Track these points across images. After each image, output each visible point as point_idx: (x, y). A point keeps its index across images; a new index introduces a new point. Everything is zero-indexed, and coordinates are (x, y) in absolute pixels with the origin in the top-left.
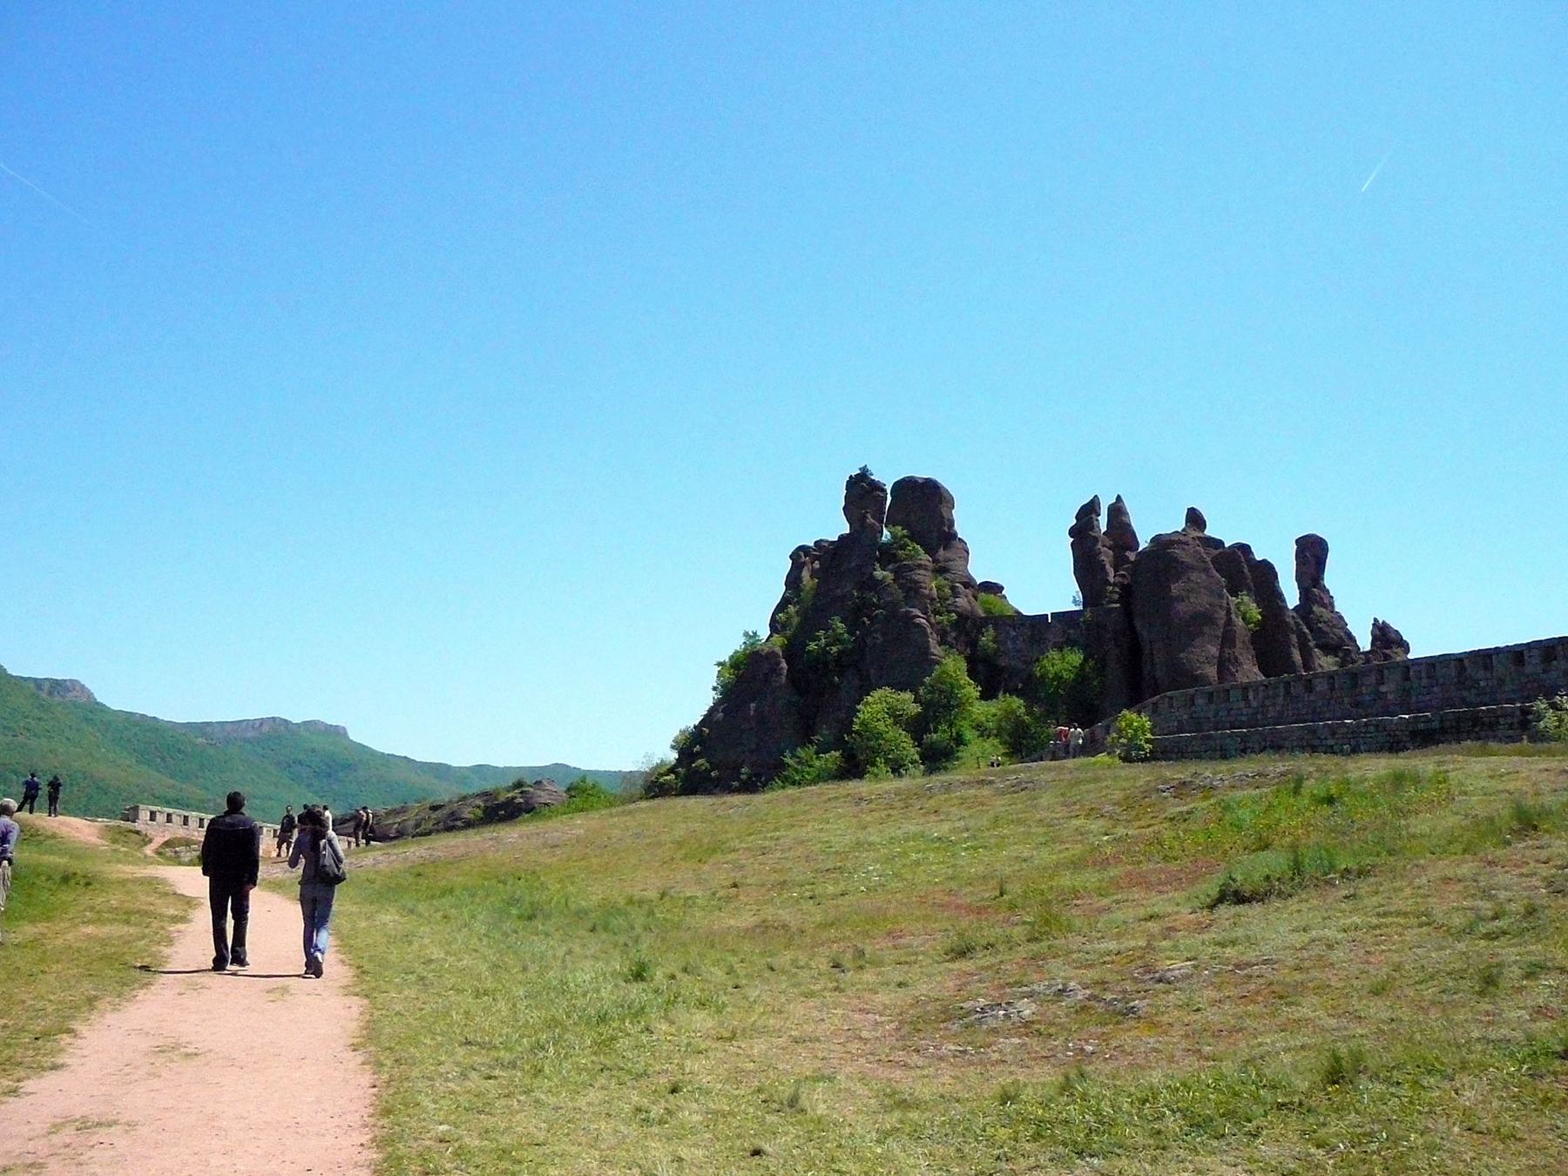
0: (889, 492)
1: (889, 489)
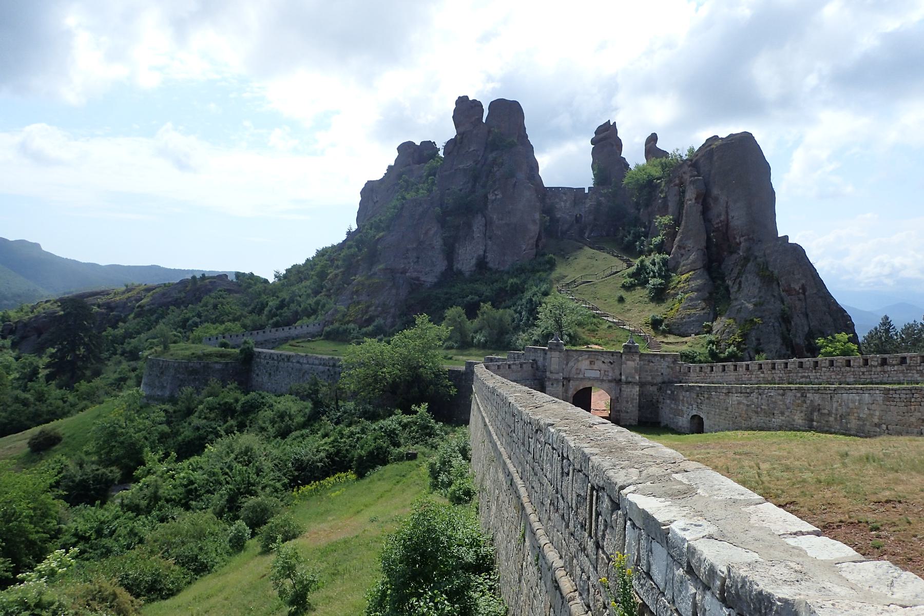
1: (486, 107)
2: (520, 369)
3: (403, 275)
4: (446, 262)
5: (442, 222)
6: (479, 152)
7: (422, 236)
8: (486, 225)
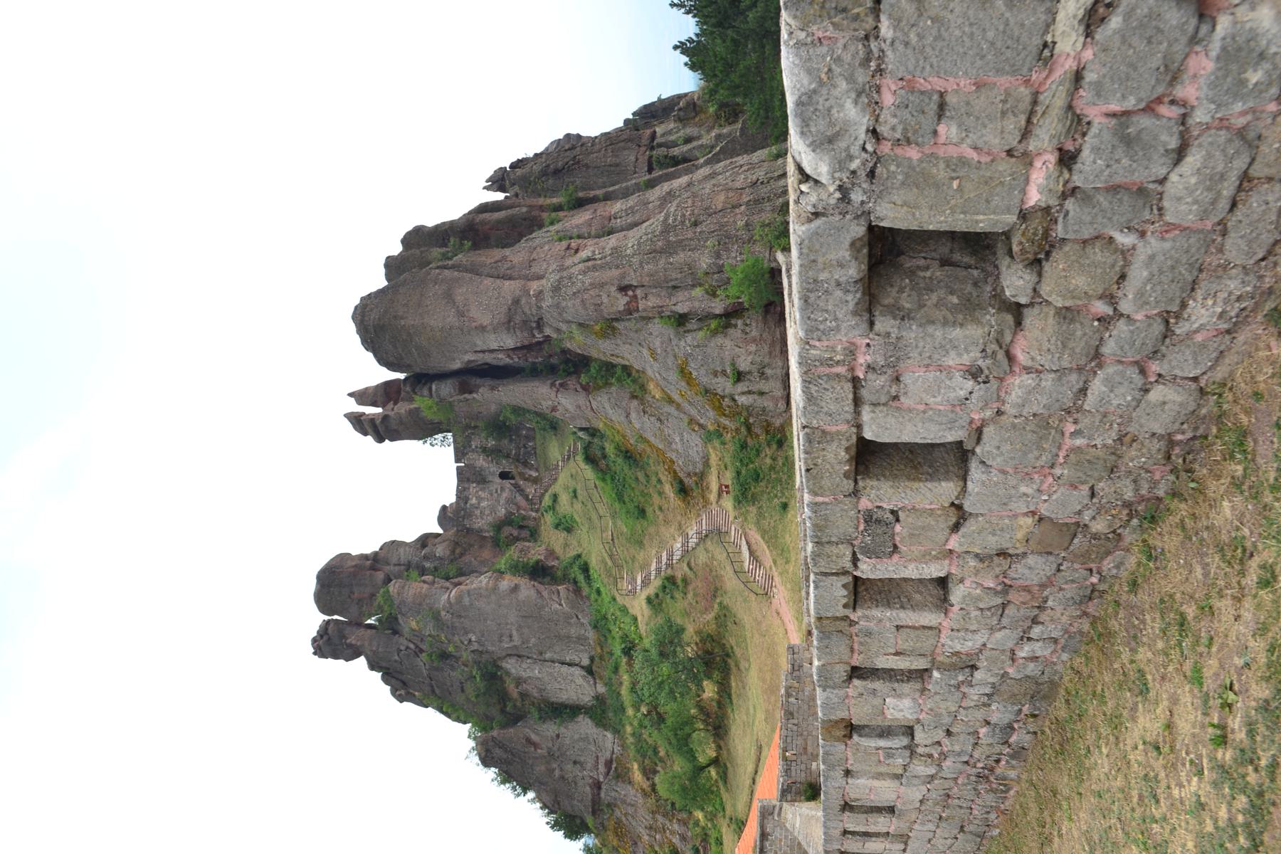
0: (330, 618)
1: (327, 618)
3: (604, 787)
6: (403, 648)
7: (539, 751)
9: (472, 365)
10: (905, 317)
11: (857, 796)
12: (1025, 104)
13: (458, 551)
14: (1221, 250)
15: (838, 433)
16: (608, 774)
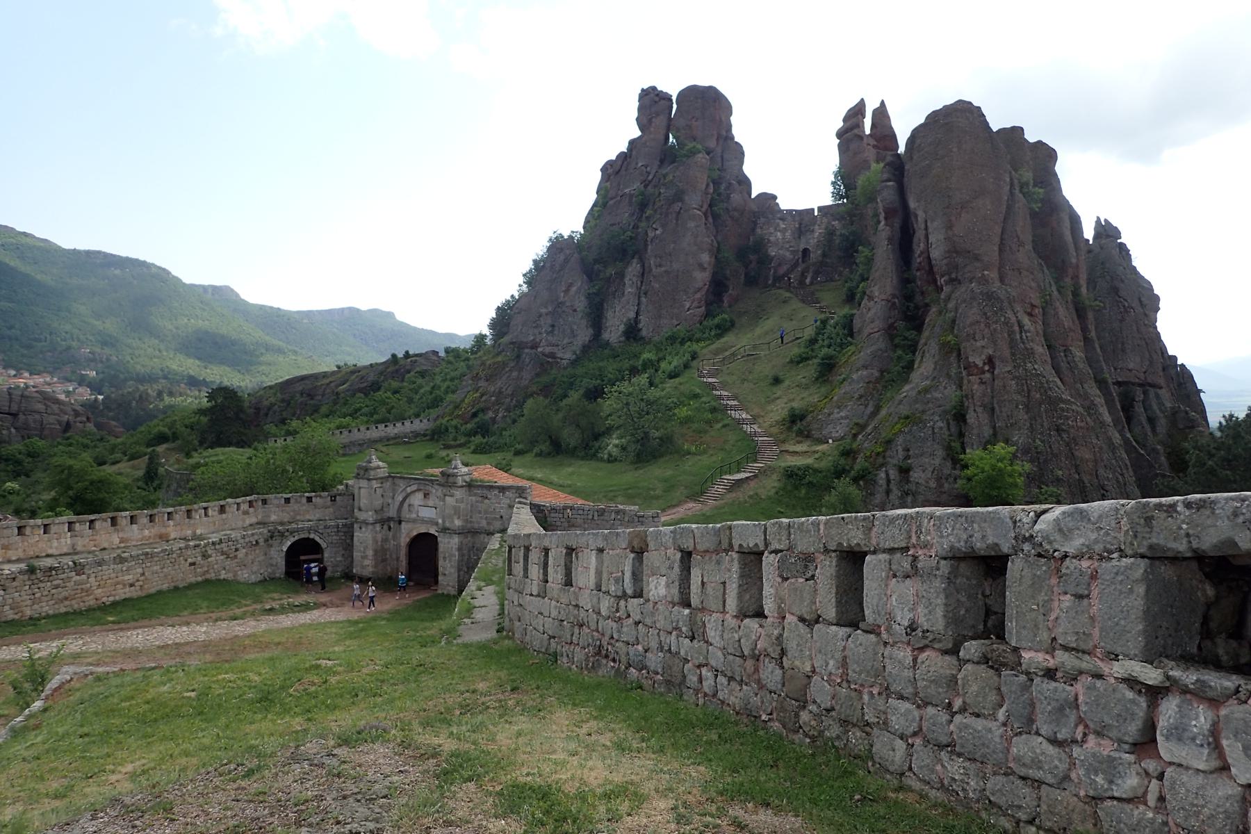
0: (674, 101)
1: (674, 99)
2: (329, 503)
4: (591, 331)
5: (590, 274)
6: (648, 169)
7: (562, 294)
8: (643, 274)
9: (913, 218)
10: (950, 580)
11: (580, 558)
12: (1083, 646)
13: (736, 214)
14: (995, 774)
15: (870, 538)
16: (544, 354)
